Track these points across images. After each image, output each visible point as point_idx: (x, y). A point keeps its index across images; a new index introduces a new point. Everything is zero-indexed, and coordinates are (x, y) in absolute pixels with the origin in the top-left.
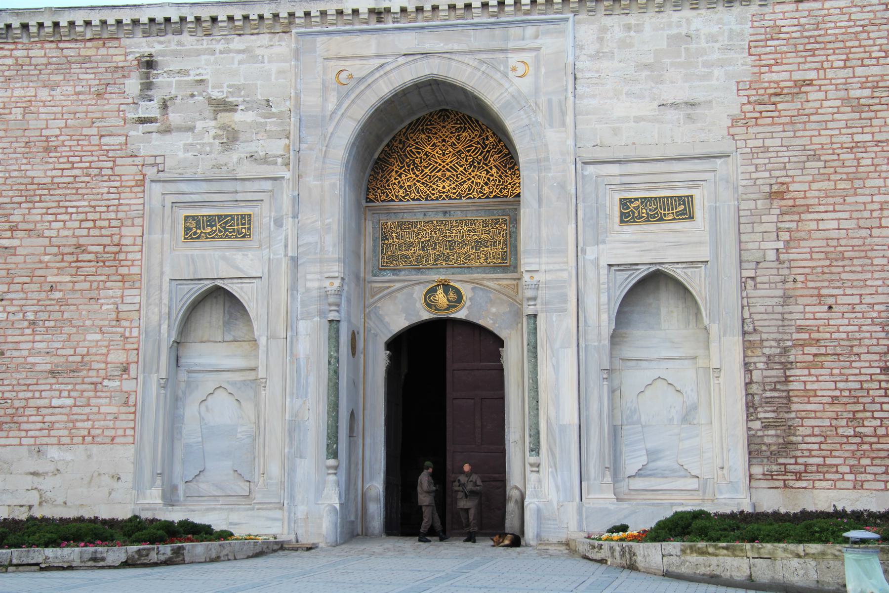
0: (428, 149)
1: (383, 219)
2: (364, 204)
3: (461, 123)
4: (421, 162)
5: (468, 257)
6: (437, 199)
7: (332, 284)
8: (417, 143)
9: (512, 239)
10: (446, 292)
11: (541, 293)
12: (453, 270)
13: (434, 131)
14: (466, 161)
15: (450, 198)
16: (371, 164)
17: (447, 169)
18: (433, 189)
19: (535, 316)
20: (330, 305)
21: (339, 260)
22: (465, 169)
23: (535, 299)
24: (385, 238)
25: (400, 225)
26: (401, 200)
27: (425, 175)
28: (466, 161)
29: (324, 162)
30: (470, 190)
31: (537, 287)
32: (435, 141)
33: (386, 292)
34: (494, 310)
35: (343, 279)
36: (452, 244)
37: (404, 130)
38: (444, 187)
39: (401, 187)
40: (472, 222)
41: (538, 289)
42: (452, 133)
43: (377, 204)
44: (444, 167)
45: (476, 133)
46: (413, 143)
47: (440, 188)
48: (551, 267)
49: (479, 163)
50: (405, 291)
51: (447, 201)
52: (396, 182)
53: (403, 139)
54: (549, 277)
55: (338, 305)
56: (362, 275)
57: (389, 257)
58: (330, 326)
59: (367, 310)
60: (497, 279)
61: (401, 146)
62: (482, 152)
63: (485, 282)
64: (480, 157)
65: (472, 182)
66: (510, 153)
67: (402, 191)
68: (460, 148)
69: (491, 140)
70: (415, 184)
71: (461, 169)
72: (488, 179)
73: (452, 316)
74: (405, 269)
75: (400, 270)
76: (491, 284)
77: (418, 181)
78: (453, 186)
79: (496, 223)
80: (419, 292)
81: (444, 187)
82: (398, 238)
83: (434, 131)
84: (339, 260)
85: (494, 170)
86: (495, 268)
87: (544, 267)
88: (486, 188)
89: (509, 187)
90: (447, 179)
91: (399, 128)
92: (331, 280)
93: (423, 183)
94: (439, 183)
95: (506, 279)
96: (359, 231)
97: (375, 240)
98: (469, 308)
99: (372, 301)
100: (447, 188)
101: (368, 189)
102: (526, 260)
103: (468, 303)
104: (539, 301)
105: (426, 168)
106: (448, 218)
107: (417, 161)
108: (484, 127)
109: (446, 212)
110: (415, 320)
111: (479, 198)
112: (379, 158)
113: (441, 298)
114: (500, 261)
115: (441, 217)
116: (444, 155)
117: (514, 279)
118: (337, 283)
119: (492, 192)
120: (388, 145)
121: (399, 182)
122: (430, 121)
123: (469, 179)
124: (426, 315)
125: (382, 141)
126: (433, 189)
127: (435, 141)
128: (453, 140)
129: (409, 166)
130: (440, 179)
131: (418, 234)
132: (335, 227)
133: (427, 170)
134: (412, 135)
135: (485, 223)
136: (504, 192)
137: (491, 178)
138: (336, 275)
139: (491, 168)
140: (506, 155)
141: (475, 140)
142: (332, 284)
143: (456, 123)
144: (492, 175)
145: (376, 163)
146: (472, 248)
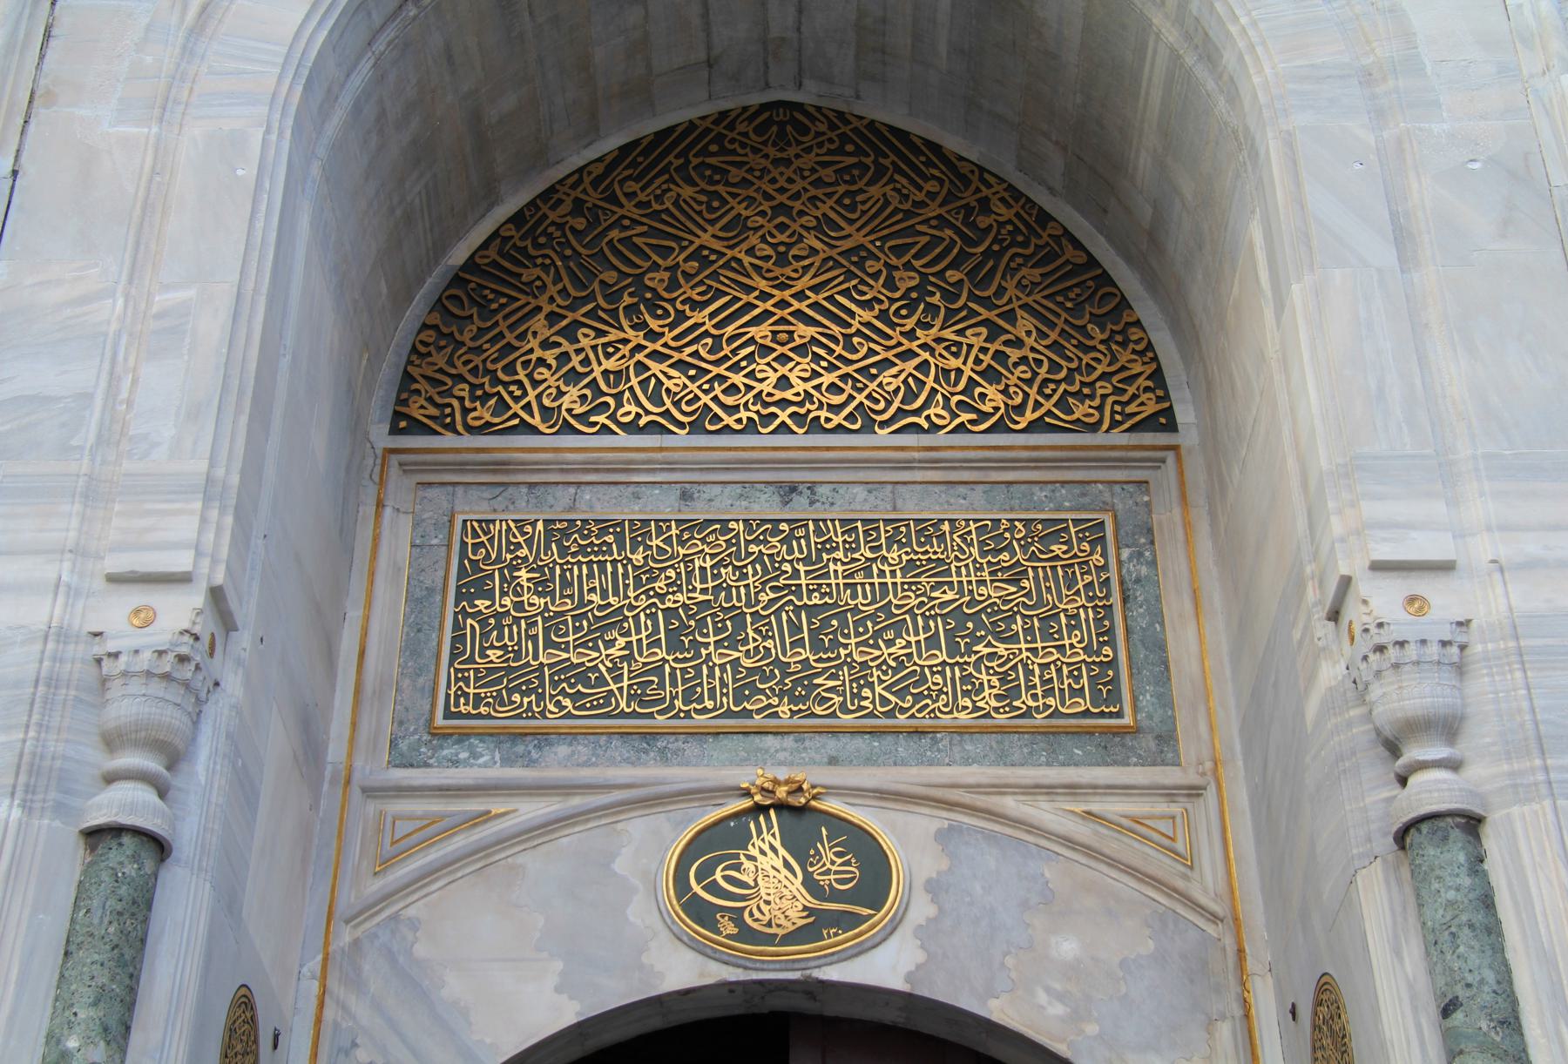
0: (705, 238)
1: (472, 507)
2: (380, 436)
3: (859, 151)
4: (673, 285)
5: (909, 683)
6: (751, 427)
7: (145, 618)
8: (655, 215)
9: (1137, 611)
10: (800, 849)
11: (1487, 693)
12: (832, 745)
13: (736, 174)
14: (890, 284)
15: (816, 426)
16: (433, 283)
17: (798, 314)
18: (733, 389)
19: (1472, 823)
20: (112, 741)
21: (210, 489)
22: (883, 316)
23: (1448, 726)
24: (473, 585)
25: (557, 533)
26: (567, 428)
27: (695, 334)
28: (890, 284)
29: (188, 52)
30: (911, 396)
31: (1455, 653)
32: (740, 209)
33: (460, 842)
34: (1067, 947)
35: (216, 595)
36: (825, 626)
37: (598, 169)
38: (784, 383)
39: (573, 377)
40: (928, 530)
41: (1460, 669)
42: (818, 183)
43: (448, 440)
44: (783, 304)
45: (931, 186)
46: (636, 213)
47: (766, 387)
48: (1531, 546)
49: (950, 296)
50: (569, 840)
51: (800, 438)
52: (550, 356)
53: (593, 198)
54: (1524, 597)
55: (174, 757)
56: (335, 752)
57: (489, 676)
58: (88, 869)
59: (345, 936)
60: (1072, 789)
61: (580, 224)
62: (963, 255)
63: (1010, 804)
64: (953, 276)
65: (924, 366)
66: (1093, 262)
67: (573, 392)
68: (859, 238)
69: (1006, 213)
70: (641, 367)
71: (867, 316)
72: (999, 356)
73: (833, 973)
74: (572, 736)
75: (544, 737)
76: (1044, 812)
77: (656, 356)
78: (828, 379)
79: (1055, 536)
80: (650, 847)
81: (784, 383)
82: (542, 586)
83: (736, 174)
84: (210, 489)
85: (1025, 325)
86: (1054, 738)
87: (1482, 549)
88: (991, 391)
89: (1103, 388)
90: (801, 350)
91: (577, 161)
92: (137, 597)
93: (680, 365)
94: (761, 364)
95: (1126, 789)
96: (342, 545)
97: (419, 600)
98: (925, 934)
99: (375, 886)
100: (800, 387)
101: (407, 377)
102: (1371, 510)
103: (922, 910)
104: (1479, 738)
105: (697, 306)
106: (800, 508)
107: (657, 280)
108: (964, 168)
109: (793, 488)
110: (614, 991)
111: (960, 428)
112: (471, 265)
113: (772, 879)
114: (1083, 704)
115: (766, 506)
116: (782, 260)
117: (1171, 793)
118: (179, 612)
119: (1020, 409)
120: (517, 219)
121: (564, 358)
122: (719, 139)
123: (907, 355)
124: (679, 968)
125: (489, 196)
126: (733, 389)
127: (740, 209)
128: (824, 208)
129: (613, 297)
130: (765, 350)
131: (645, 576)
132: (212, 326)
133: (698, 317)
134: (631, 186)
135: (993, 537)
136: (1080, 410)
137: (1014, 354)
138: (181, 561)
139: (1010, 316)
140: (1077, 269)
141: (933, 211)
142: (145, 618)
143: (840, 151)
144: (1018, 343)
145: (457, 280)
146: (933, 642)
